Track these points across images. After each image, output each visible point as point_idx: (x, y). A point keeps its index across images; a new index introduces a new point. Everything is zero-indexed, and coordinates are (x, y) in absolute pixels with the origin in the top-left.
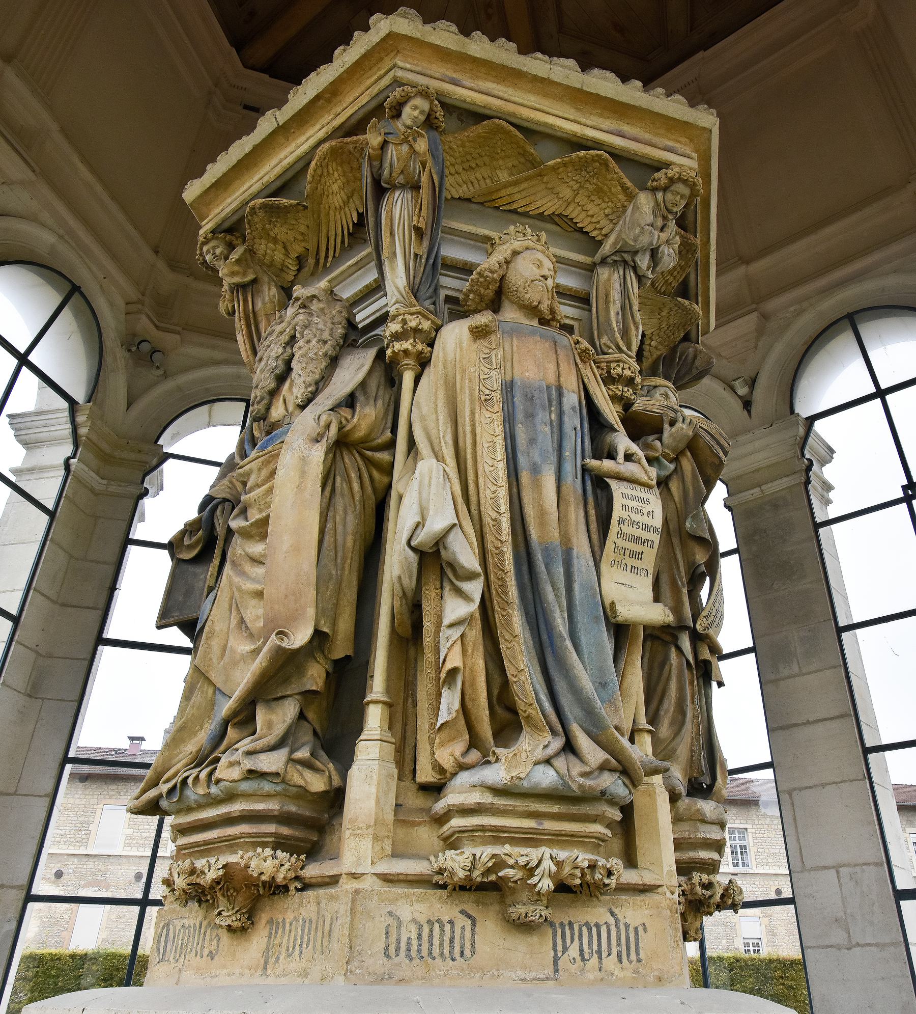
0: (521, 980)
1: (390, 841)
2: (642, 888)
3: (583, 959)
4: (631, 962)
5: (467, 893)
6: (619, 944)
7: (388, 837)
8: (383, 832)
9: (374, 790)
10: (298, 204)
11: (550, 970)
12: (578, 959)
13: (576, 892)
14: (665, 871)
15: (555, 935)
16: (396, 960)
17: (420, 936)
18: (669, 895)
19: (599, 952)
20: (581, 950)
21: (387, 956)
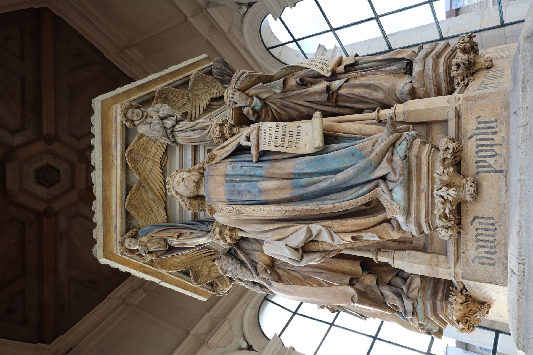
0: (506, 192)
1: (439, 256)
2: (457, 118)
3: (495, 155)
4: (497, 126)
5: (462, 220)
6: (487, 133)
7: (437, 257)
8: (435, 261)
9: (415, 265)
10: (191, 269)
11: (502, 175)
12: (495, 158)
13: (460, 159)
14: (448, 105)
15: (483, 172)
16: (496, 260)
17: (484, 247)
18: (460, 102)
19: (492, 145)
20: (491, 156)
21: (494, 264)
